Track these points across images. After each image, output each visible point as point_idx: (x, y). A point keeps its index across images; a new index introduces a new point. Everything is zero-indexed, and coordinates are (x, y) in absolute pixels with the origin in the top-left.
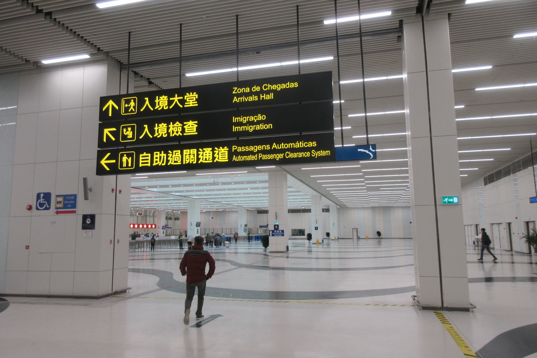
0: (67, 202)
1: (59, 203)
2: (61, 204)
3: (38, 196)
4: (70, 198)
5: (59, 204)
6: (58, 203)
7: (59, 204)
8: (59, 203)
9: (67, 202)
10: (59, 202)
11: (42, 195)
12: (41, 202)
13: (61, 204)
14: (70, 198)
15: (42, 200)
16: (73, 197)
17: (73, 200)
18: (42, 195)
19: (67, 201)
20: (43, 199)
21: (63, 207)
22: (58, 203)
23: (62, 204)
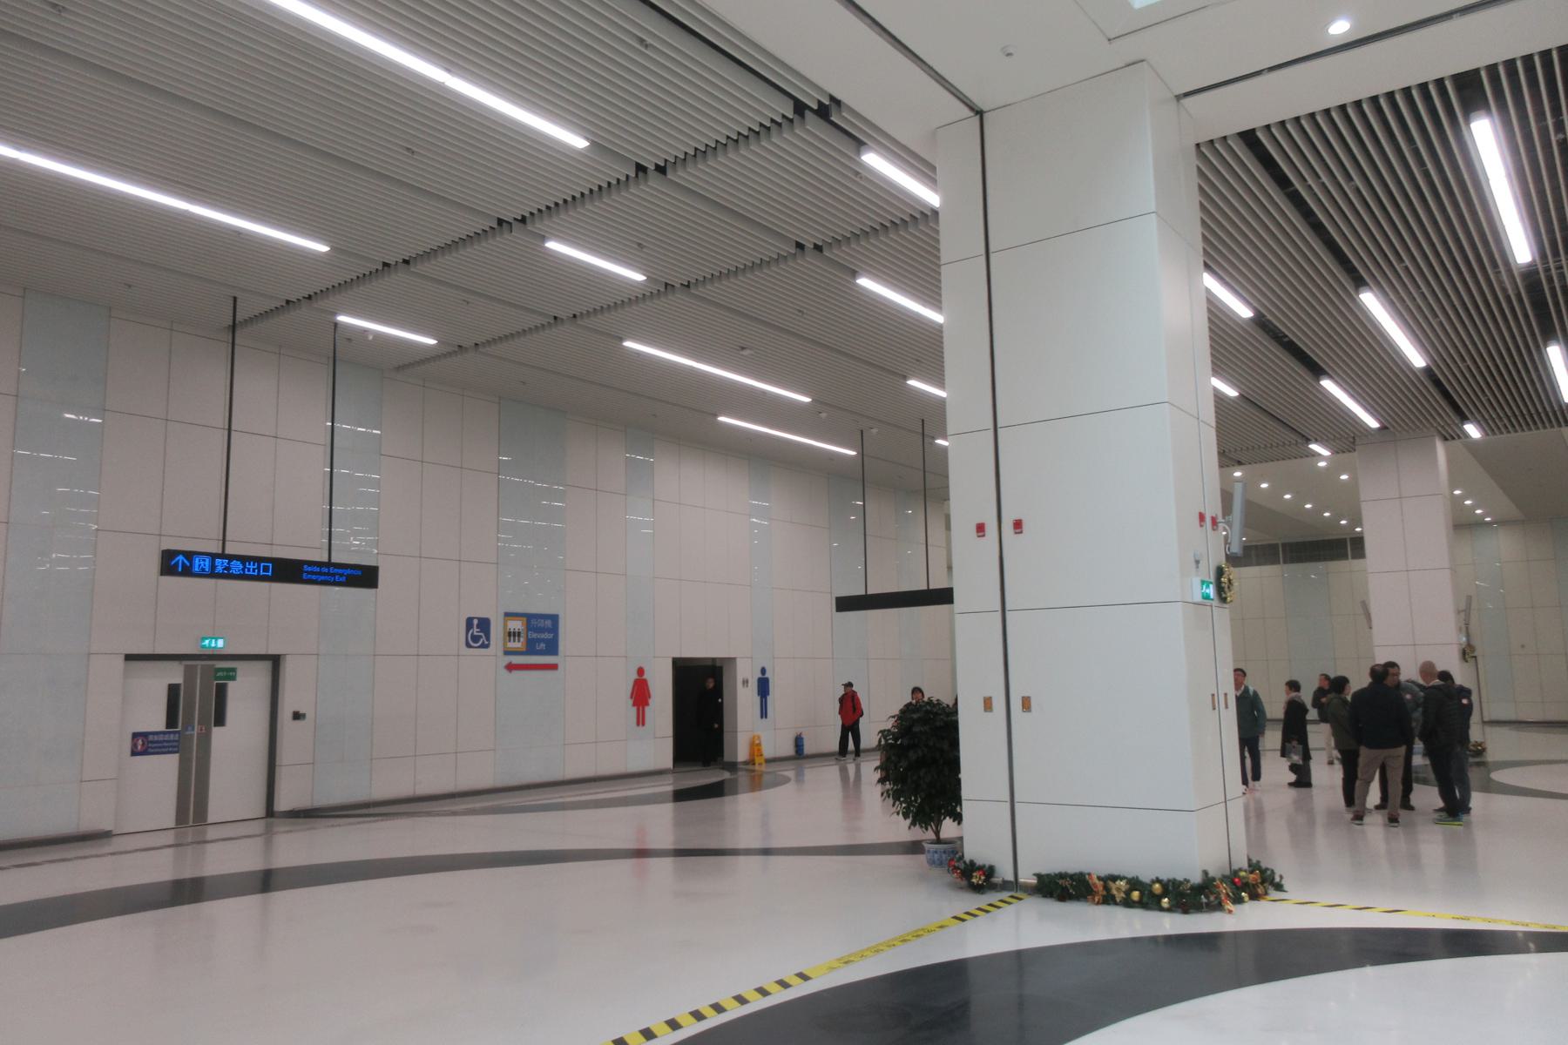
0: (535, 636)
1: (514, 636)
2: (519, 641)
3: (469, 622)
4: (541, 623)
5: (514, 641)
6: (512, 638)
7: (514, 641)
8: (514, 636)
9: (535, 636)
10: (512, 635)
11: (476, 622)
12: (475, 634)
13: (519, 641)
14: (542, 625)
15: (476, 630)
16: (549, 623)
17: (549, 631)
18: (476, 622)
19: (535, 632)
20: (478, 628)
21: (524, 650)
22: (512, 638)
23: (522, 639)
